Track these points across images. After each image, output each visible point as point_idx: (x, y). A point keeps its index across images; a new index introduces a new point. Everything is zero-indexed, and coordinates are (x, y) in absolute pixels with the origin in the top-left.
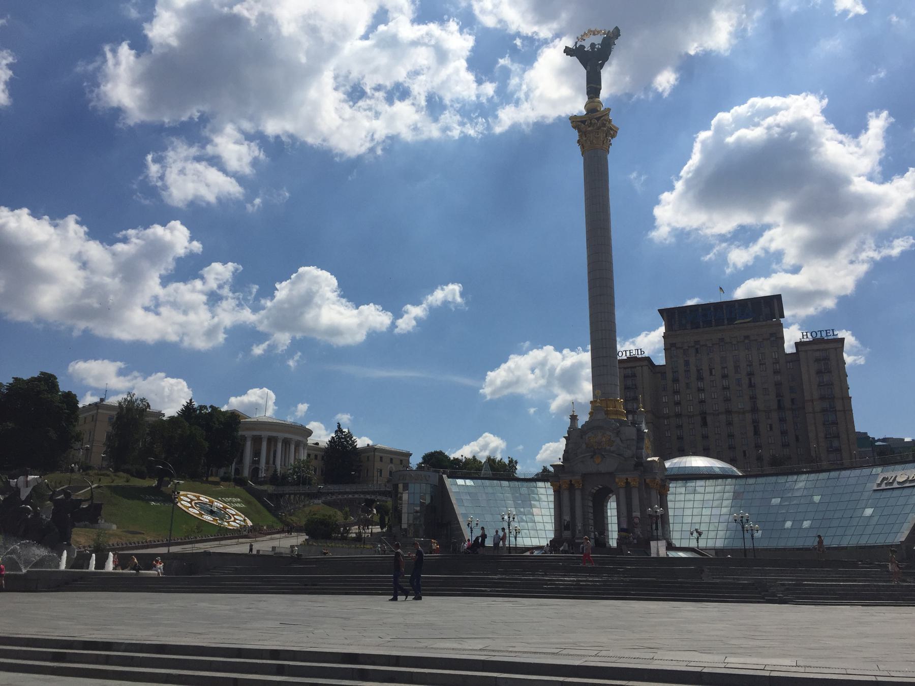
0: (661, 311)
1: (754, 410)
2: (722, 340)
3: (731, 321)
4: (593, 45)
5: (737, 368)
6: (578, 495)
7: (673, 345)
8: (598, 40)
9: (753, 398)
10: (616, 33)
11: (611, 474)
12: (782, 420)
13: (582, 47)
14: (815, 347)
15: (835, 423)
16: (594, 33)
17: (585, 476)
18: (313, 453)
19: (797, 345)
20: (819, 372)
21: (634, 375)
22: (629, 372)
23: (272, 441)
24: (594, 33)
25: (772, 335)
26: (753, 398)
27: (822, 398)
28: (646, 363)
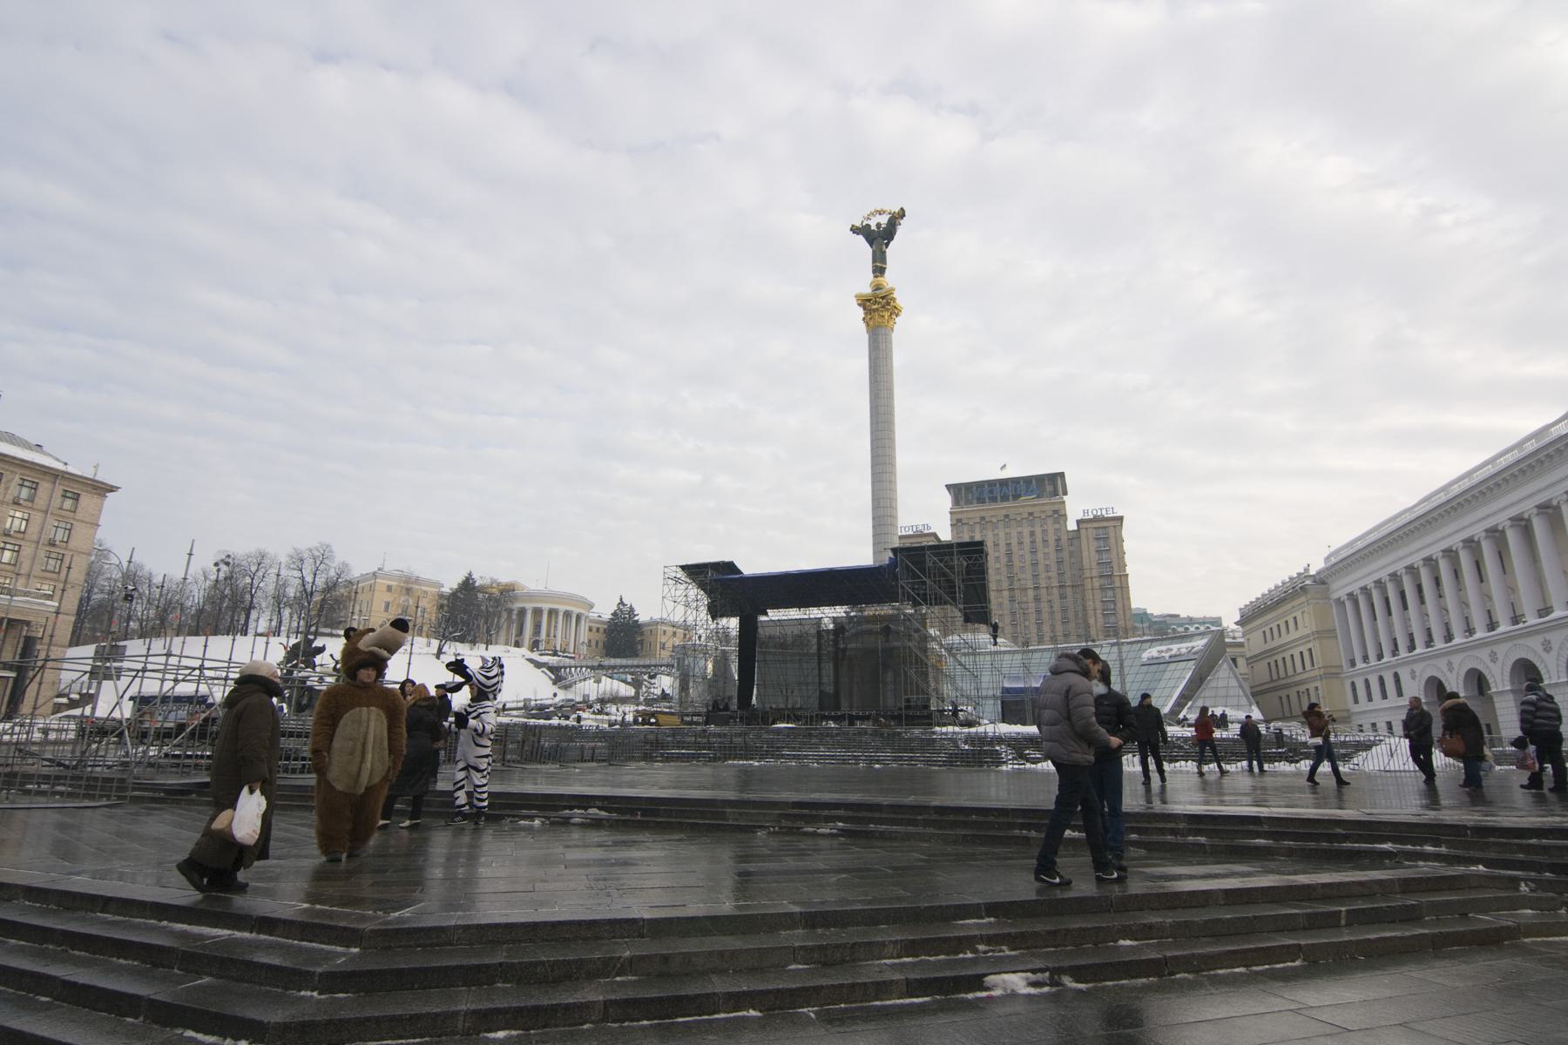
0: (948, 487)
1: (1036, 588)
2: (1007, 516)
3: (1016, 497)
4: (878, 225)
5: (1021, 543)
7: (959, 521)
8: (884, 220)
10: (902, 214)
12: (1063, 597)
13: (868, 226)
16: (880, 213)
18: (595, 626)
19: (1078, 522)
23: (553, 613)
24: (880, 213)
25: (1055, 512)
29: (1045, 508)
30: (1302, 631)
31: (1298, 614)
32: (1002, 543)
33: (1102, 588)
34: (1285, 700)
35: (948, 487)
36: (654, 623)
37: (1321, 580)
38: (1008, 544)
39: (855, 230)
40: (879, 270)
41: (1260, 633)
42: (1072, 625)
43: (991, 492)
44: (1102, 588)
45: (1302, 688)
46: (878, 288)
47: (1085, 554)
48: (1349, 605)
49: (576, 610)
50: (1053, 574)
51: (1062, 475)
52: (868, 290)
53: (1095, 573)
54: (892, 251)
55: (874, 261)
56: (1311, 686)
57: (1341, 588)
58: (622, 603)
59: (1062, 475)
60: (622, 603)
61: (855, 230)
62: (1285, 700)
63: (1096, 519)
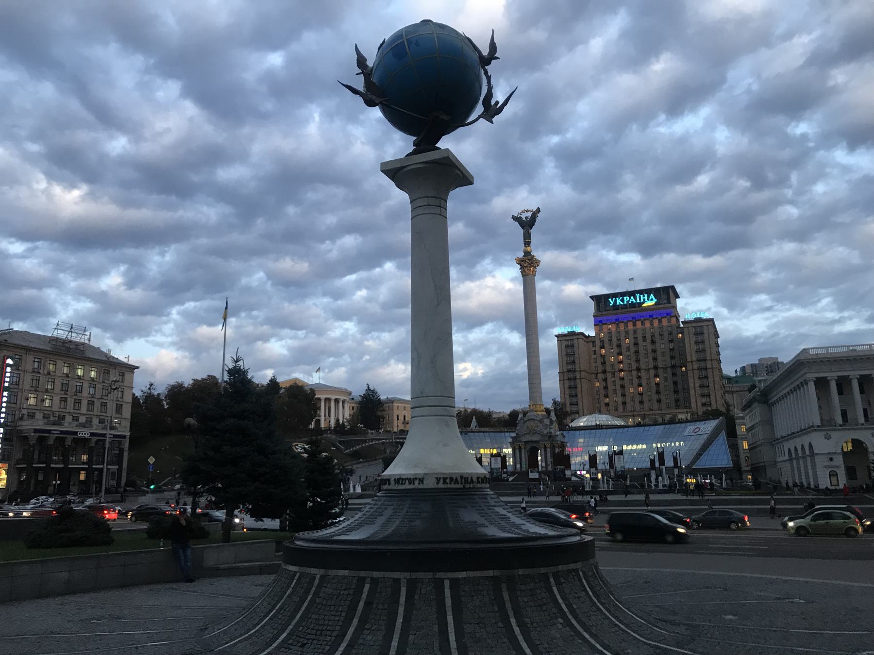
0: (592, 297)
4: (526, 218)
6: (523, 450)
7: (601, 322)
8: (529, 214)
9: (655, 359)
11: (538, 442)
14: (694, 325)
15: (706, 377)
17: (526, 442)
20: (697, 343)
21: (573, 346)
22: (569, 343)
26: (655, 359)
27: (698, 361)
33: (700, 369)
35: (592, 297)
36: (391, 401)
38: (636, 338)
39: (514, 218)
40: (527, 243)
42: (681, 396)
44: (700, 369)
46: (527, 254)
47: (687, 345)
49: (342, 398)
50: (668, 358)
51: (673, 288)
52: (521, 255)
53: (694, 359)
54: (533, 231)
55: (524, 239)
58: (369, 389)
60: (369, 389)
61: (514, 218)
63: (698, 320)
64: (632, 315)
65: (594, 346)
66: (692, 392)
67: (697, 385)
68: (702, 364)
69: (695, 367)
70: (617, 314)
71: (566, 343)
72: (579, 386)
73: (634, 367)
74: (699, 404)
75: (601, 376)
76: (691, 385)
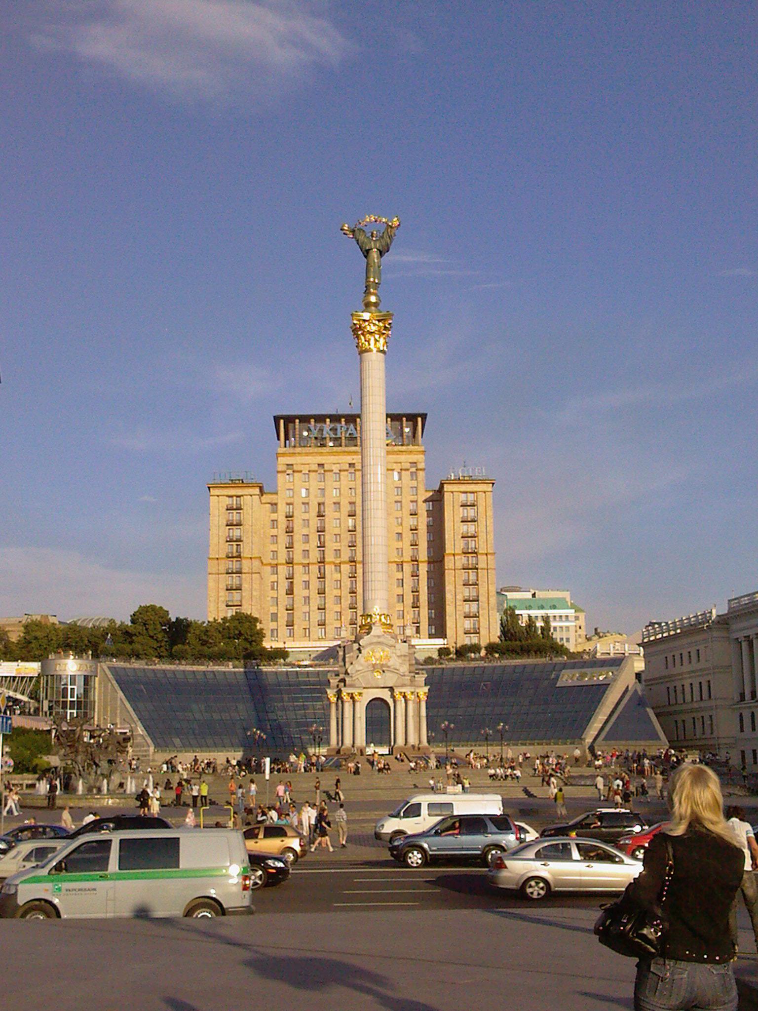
14: (463, 488)
19: (442, 485)
28: (257, 491)
29: (402, 458)
30: (702, 665)
31: (701, 648)
32: (345, 503)
34: (680, 724)
37: (724, 622)
41: (663, 656)
43: (334, 430)
45: (697, 715)
48: (745, 645)
51: (424, 417)
56: (706, 715)
57: (741, 629)
59: (424, 417)
62: (680, 724)
64: (349, 459)
65: (275, 511)
66: (449, 609)
67: (460, 597)
68: (472, 560)
69: (459, 565)
70: (321, 454)
71: (228, 501)
72: (245, 586)
73: (346, 555)
74: (461, 632)
75: (283, 570)
76: (449, 597)
